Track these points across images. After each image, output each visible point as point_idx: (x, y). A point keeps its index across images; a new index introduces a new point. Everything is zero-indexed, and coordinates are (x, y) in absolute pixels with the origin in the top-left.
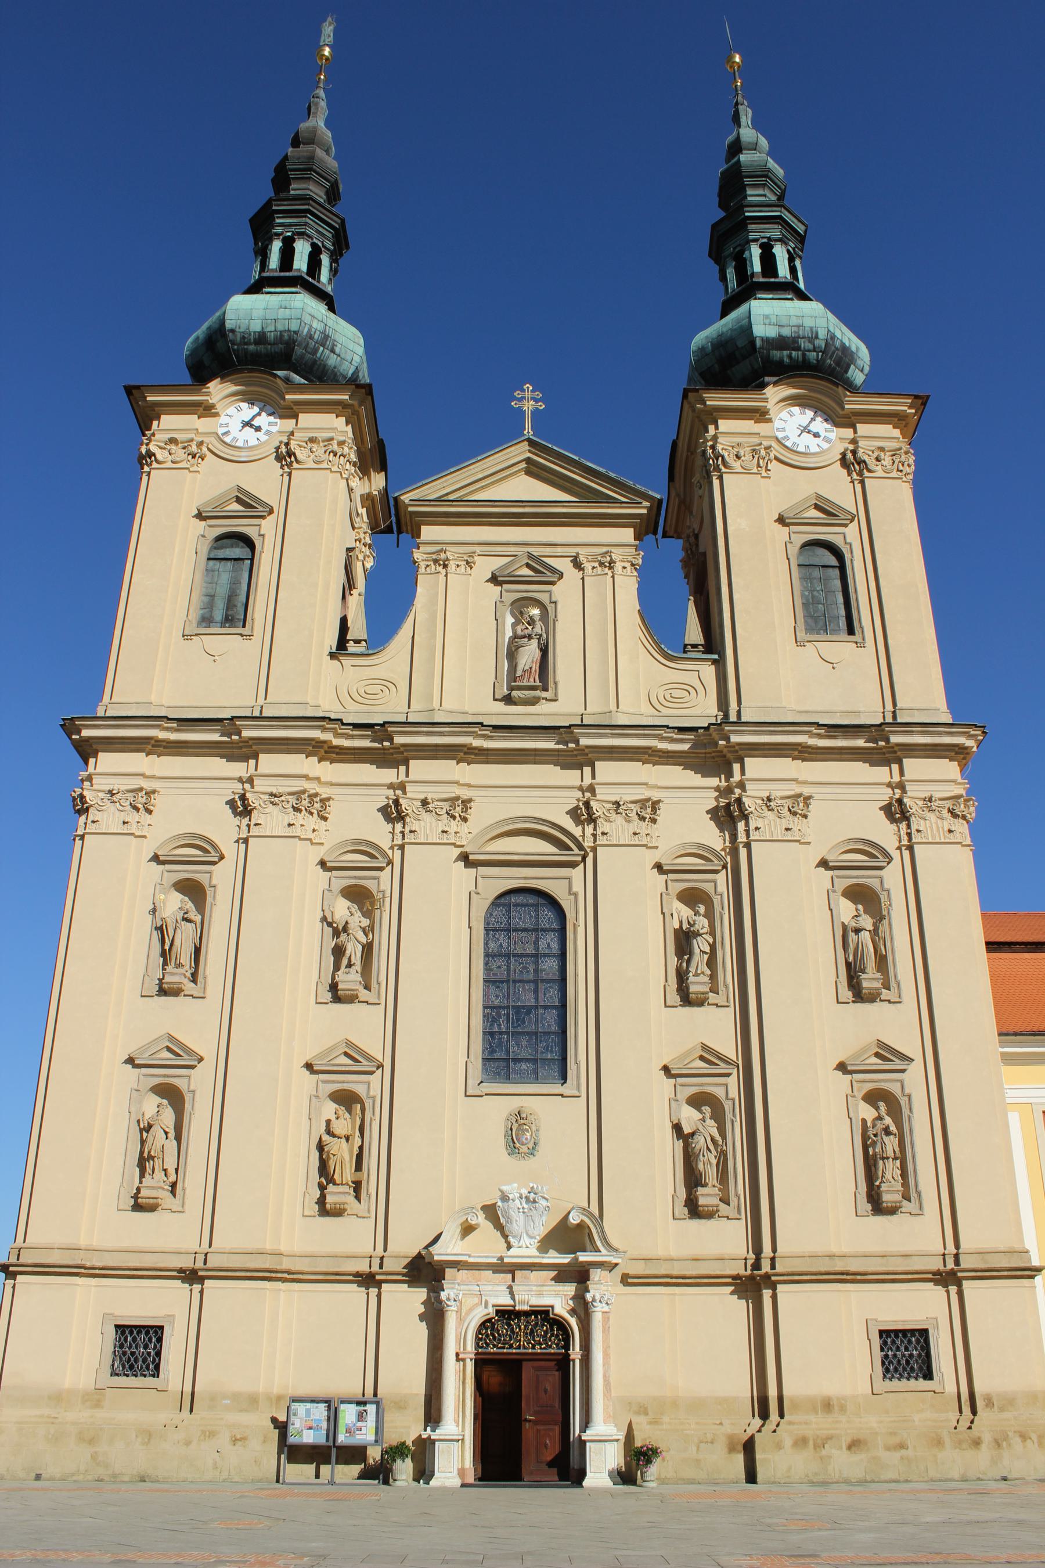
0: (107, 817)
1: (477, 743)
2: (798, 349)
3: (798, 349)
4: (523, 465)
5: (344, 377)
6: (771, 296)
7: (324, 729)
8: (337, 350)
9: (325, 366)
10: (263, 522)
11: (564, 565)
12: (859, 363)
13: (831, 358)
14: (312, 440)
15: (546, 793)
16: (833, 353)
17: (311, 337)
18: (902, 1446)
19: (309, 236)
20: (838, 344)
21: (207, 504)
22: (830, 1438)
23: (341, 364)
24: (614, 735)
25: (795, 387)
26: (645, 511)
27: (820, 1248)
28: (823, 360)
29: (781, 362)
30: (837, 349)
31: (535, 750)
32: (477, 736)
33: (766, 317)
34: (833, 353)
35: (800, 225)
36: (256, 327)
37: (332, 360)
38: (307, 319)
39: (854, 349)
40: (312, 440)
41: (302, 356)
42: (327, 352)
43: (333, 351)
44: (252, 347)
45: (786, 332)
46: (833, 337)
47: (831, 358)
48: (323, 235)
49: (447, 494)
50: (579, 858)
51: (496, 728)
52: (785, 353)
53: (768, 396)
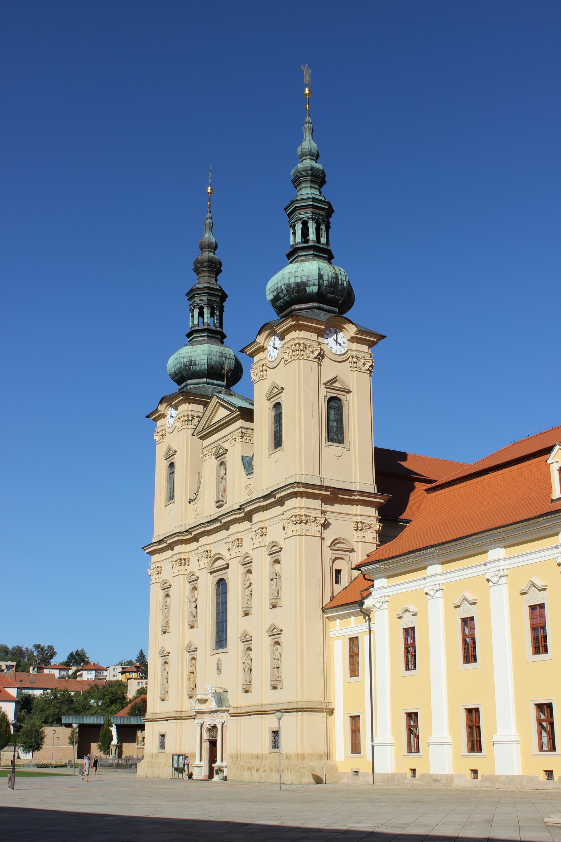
0: (154, 578)
1: (207, 529)
2: (281, 298)
3: (281, 298)
4: (218, 404)
5: (205, 370)
6: (295, 257)
7: (179, 536)
8: (197, 363)
9: (197, 371)
10: (175, 456)
11: (226, 445)
12: (311, 283)
13: (293, 293)
14: (179, 419)
15: (217, 543)
16: (293, 291)
17: (185, 366)
18: (265, 771)
19: (197, 306)
20: (293, 286)
21: (164, 455)
22: (253, 768)
23: (201, 367)
24: (251, 505)
25: (267, 330)
26: (239, 413)
27: (259, 702)
28: (291, 297)
29: (281, 306)
30: (294, 288)
31: (229, 521)
32: (205, 527)
33: (269, 289)
34: (293, 291)
35: (308, 200)
36: (173, 371)
37: (198, 368)
38: (182, 360)
39: (304, 279)
40: (179, 419)
41: (187, 374)
42: (194, 367)
43: (196, 365)
44: (176, 378)
45: (275, 293)
46: (289, 285)
47: (293, 293)
48: (202, 300)
49: (204, 426)
50: (227, 566)
51: (207, 522)
52: (279, 302)
53: (258, 341)
